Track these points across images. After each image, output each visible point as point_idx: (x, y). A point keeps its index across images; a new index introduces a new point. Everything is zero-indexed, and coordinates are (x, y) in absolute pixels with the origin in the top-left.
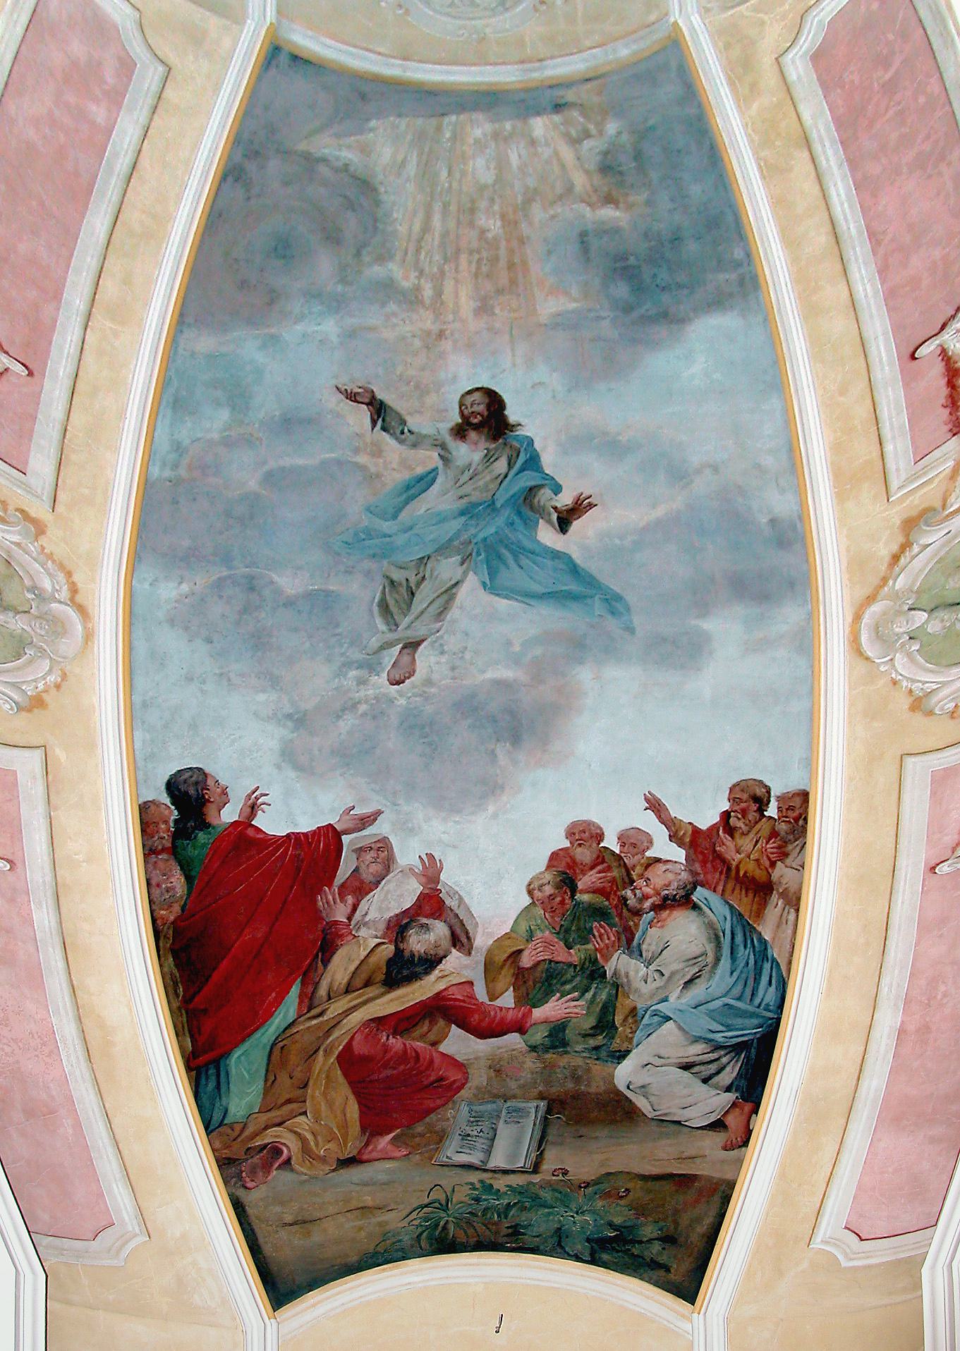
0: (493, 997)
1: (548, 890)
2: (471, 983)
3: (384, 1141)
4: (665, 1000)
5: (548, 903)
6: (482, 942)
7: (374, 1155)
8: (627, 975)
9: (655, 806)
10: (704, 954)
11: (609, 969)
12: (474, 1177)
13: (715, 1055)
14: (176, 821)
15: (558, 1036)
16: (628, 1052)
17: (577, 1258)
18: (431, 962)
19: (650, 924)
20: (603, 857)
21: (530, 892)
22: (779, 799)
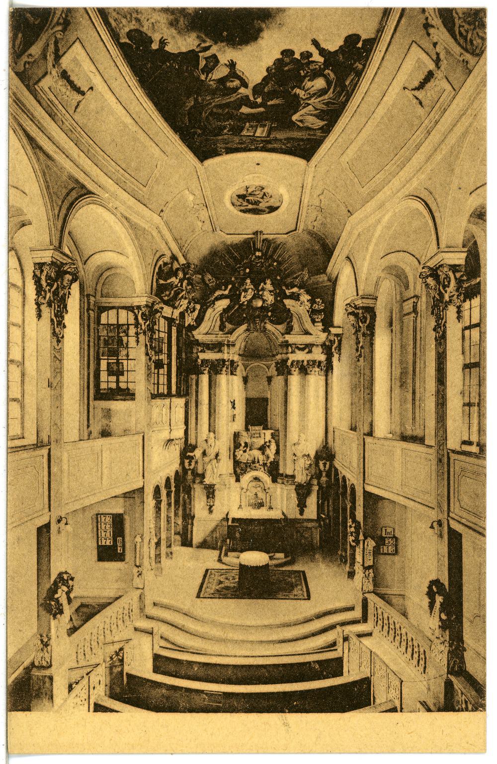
0: (255, 99)
6: (251, 86)
9: (315, 43)
12: (251, 138)
18: (236, 90)
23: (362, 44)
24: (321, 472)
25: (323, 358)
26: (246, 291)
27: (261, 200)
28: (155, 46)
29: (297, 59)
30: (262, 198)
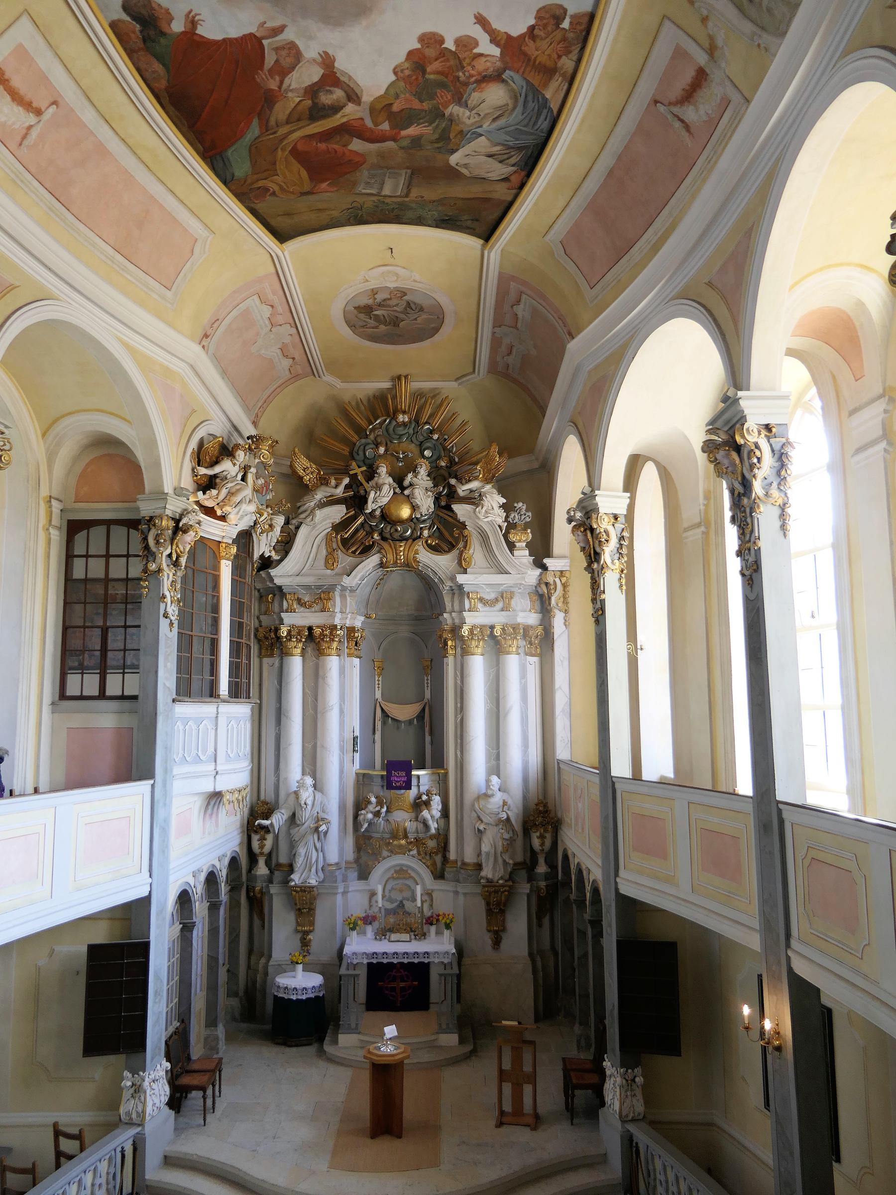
0: (376, 124)
1: (407, 72)
2: (362, 119)
3: (324, 185)
4: (481, 126)
5: (407, 80)
6: (367, 98)
7: (319, 190)
8: (458, 115)
9: (481, 21)
10: (507, 105)
11: (447, 112)
12: (375, 198)
13: (508, 151)
14: (141, 32)
15: (416, 142)
16: (457, 150)
17: (429, 226)
18: (336, 109)
19: (474, 90)
20: (444, 53)
21: (395, 73)
22: (572, 17)
23: (571, 23)
24: (533, 852)
25: (529, 618)
26: (379, 488)
27: (402, 316)
28: (178, 26)
29: (450, 51)
30: (405, 312)
